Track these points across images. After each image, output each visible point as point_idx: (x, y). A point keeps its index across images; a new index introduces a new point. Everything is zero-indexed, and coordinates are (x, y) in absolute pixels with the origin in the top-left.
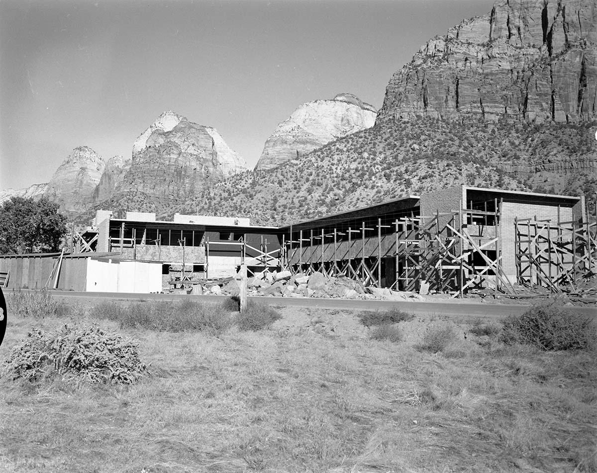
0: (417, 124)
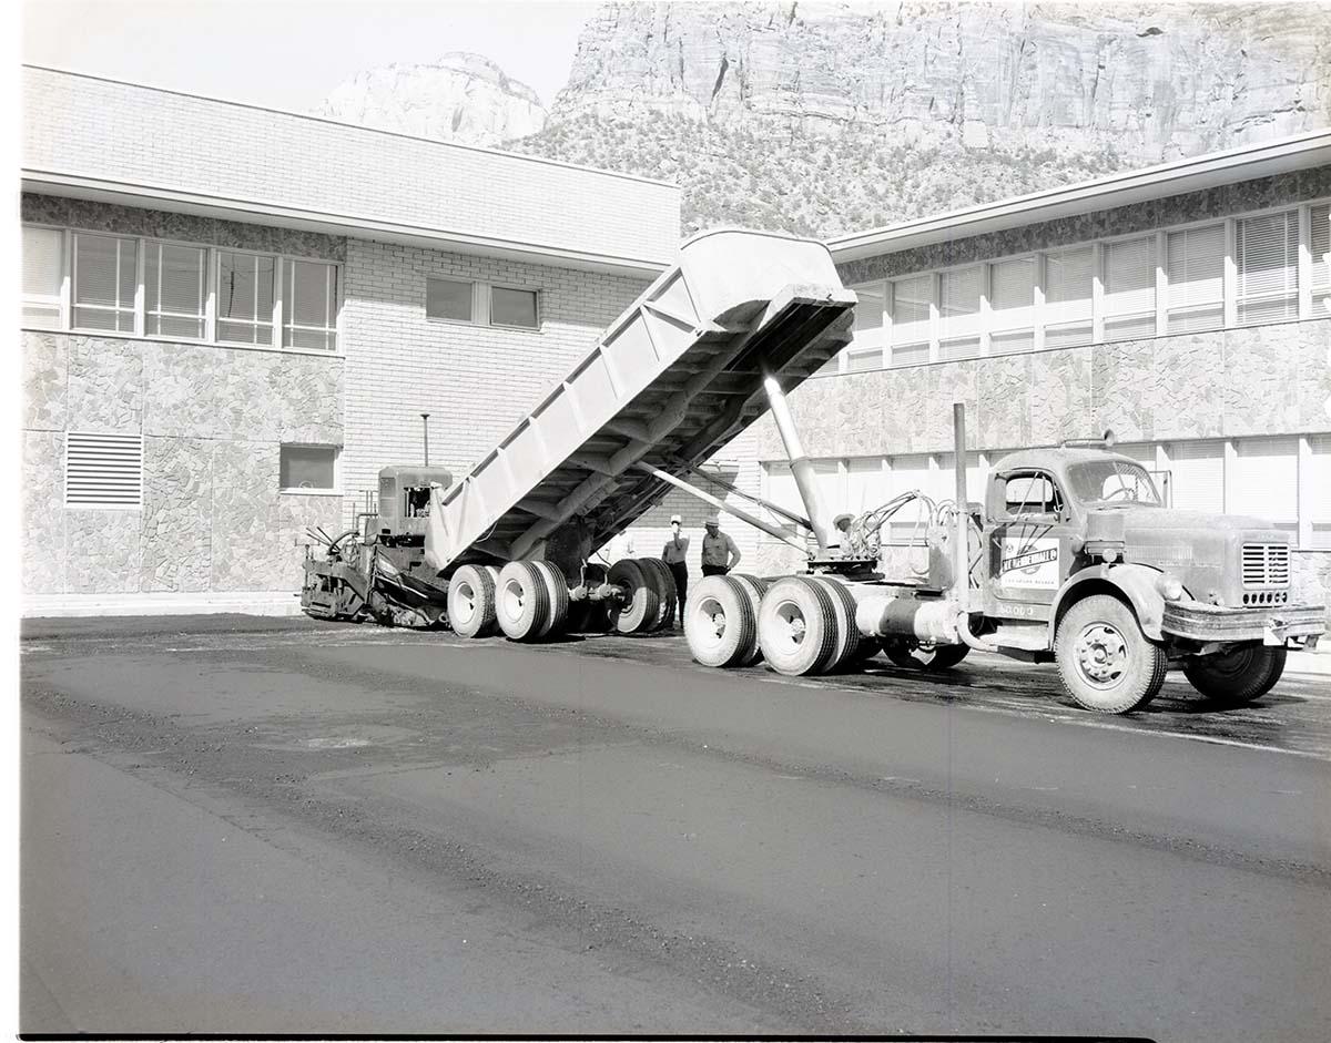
0: (653, 131)
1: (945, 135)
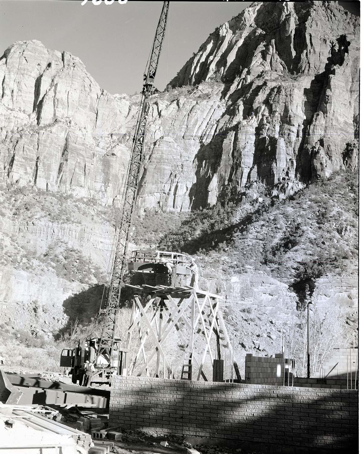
1: (28, 181)
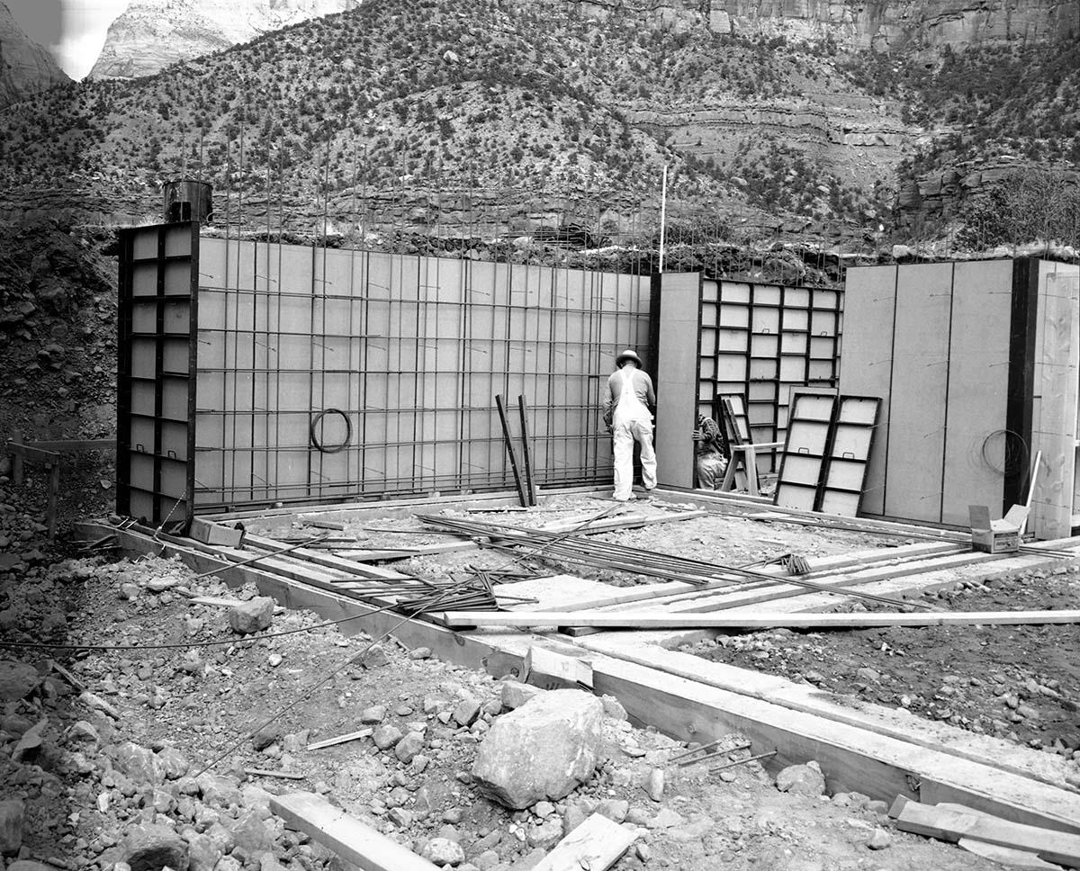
1: (694, 21)
